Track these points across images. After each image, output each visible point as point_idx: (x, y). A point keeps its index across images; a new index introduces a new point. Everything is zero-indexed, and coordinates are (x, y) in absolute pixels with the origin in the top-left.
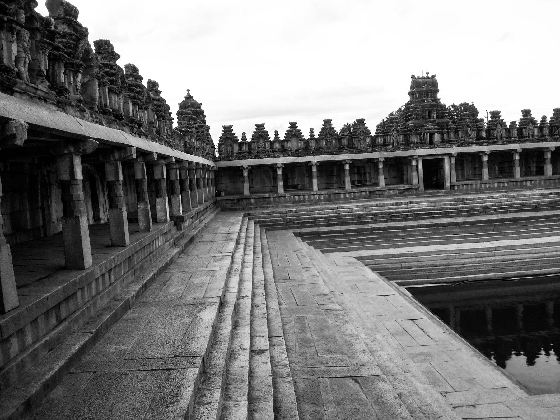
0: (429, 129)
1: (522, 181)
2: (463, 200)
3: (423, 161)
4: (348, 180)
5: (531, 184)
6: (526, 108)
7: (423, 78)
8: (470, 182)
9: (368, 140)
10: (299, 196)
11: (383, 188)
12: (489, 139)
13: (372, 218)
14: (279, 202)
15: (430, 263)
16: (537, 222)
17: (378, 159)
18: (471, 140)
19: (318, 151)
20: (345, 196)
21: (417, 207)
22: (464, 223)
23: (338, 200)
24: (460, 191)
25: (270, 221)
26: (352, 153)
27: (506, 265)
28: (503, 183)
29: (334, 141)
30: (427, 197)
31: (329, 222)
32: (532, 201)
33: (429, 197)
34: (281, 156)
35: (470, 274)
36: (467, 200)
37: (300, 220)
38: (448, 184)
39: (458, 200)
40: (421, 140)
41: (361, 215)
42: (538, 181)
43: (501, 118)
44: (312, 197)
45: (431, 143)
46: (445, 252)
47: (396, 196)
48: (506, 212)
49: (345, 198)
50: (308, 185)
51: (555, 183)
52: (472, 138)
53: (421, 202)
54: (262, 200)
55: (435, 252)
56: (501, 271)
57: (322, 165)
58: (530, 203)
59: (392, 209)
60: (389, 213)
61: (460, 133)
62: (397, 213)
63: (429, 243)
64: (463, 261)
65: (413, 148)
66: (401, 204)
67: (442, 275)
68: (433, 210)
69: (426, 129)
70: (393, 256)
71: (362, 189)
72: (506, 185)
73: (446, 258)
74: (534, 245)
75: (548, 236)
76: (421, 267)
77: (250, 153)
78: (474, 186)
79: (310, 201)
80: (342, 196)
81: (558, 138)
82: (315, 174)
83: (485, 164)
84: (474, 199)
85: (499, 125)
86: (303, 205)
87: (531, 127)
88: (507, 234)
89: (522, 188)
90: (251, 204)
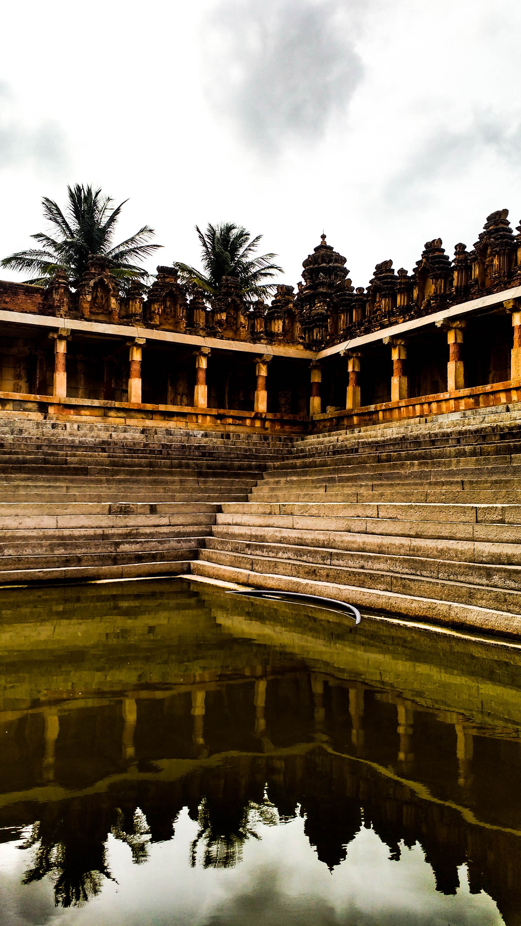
10: (422, 404)
54: (367, 418)
77: (360, 324)
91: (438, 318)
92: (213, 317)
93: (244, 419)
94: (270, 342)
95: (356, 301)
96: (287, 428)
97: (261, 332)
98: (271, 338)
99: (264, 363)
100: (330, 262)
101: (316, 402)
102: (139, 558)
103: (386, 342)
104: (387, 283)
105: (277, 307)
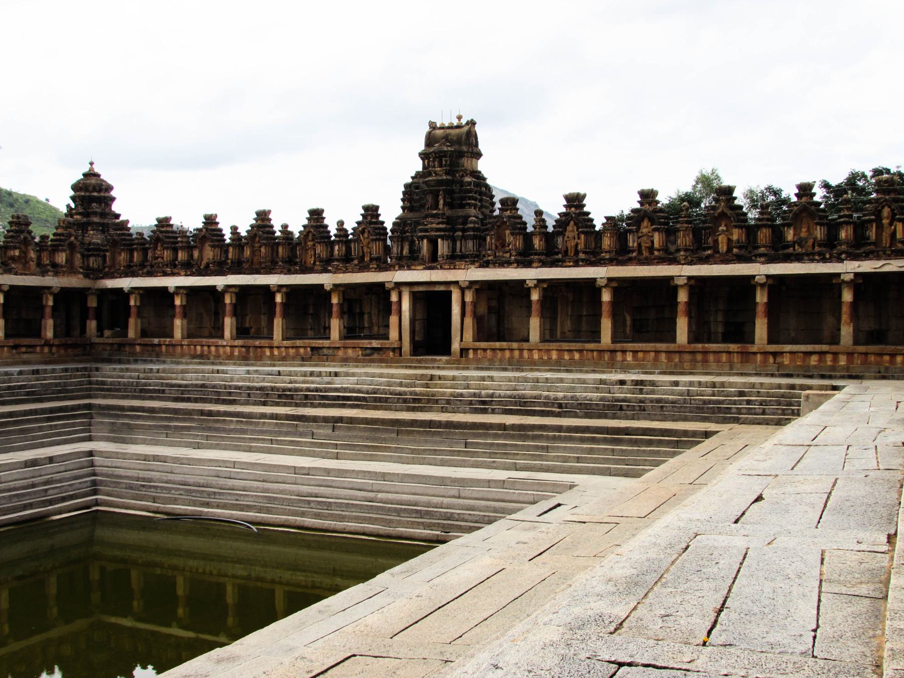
0: (426, 231)
1: (613, 352)
2: (432, 378)
3: (415, 297)
4: (278, 323)
5: (635, 358)
6: (647, 187)
7: (451, 127)
8: (497, 345)
9: (318, 250)
11: (333, 343)
12: (547, 255)
13: (249, 395)
14: (173, 355)
15: (178, 478)
16: (486, 436)
17: (322, 286)
18: (508, 255)
19: (238, 268)
20: (272, 353)
21: (338, 382)
22: (351, 420)
23: (259, 358)
24: (478, 361)
25: (111, 383)
26: (289, 272)
27: (290, 502)
28: (570, 351)
29: (263, 250)
30: (406, 367)
31: (183, 393)
32: (561, 395)
33: (410, 367)
34: (183, 273)
35: (218, 507)
36: (440, 378)
37: (150, 385)
38: (456, 346)
39: (422, 377)
40: (411, 251)
41: (239, 388)
42: (652, 354)
43: (585, 209)
44: (221, 350)
45: (433, 262)
46: (224, 463)
47: (356, 360)
48: (484, 411)
49: (272, 357)
50: (265, 330)
51: (694, 361)
52: (509, 251)
53: (353, 375)
54: (150, 348)
55: (210, 460)
56: (268, 511)
57: (244, 292)
58: (556, 399)
59: (296, 382)
60: (284, 390)
61: (488, 238)
62: (297, 390)
63: (251, 447)
64: (231, 483)
65: (395, 270)
66: (320, 374)
67: (175, 501)
68: (359, 391)
69: (421, 230)
70: (146, 458)
71: (298, 343)
72: (577, 356)
73: (214, 473)
74: (384, 476)
75: (473, 466)
76: (166, 482)
77: (142, 265)
78: (507, 354)
79: (218, 356)
80: (268, 353)
81: (708, 257)
82: (228, 309)
83: (535, 308)
84: (454, 378)
85: (572, 223)
86: (200, 363)
87: (645, 231)
88: (401, 450)
89: (612, 366)
90: (133, 354)
91: (219, 282)
92: (5, 253)
93: (34, 346)
94: (56, 274)
95: (137, 244)
96: (69, 350)
97: (47, 265)
98: (56, 269)
99: (51, 293)
100: (100, 191)
101: (92, 325)
102: (64, 499)
103: (171, 290)
104: (168, 237)
105: (60, 240)
